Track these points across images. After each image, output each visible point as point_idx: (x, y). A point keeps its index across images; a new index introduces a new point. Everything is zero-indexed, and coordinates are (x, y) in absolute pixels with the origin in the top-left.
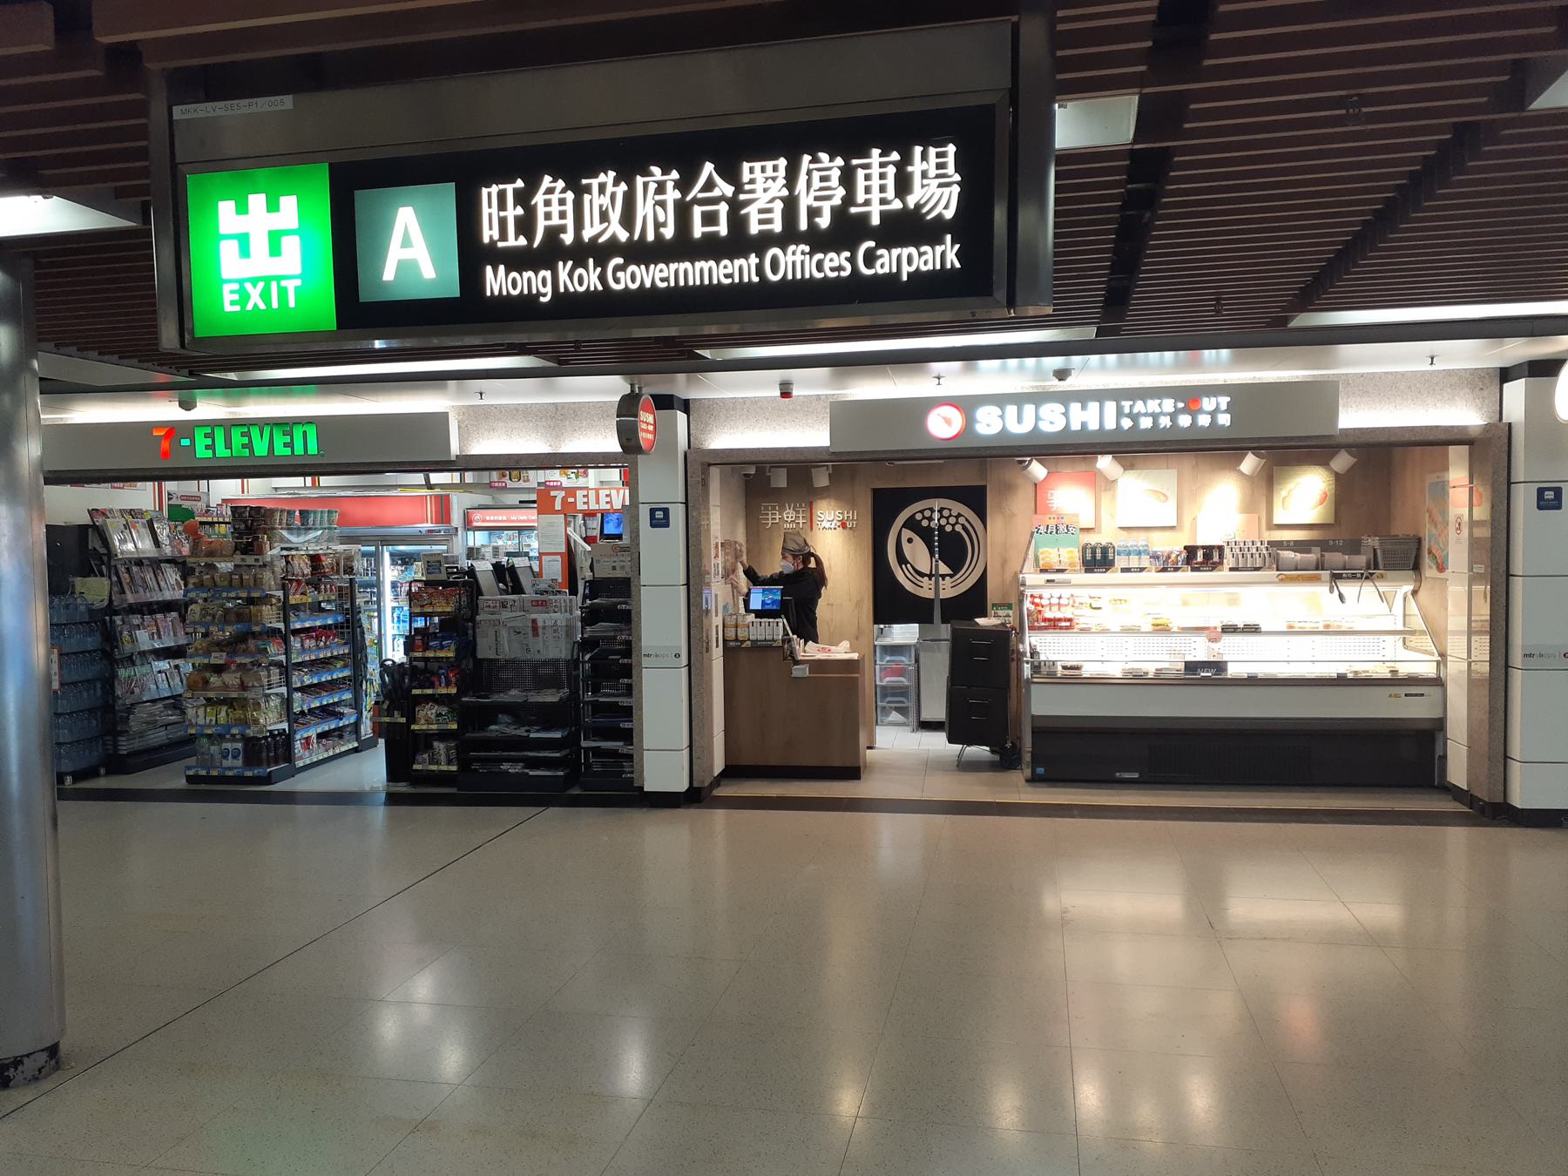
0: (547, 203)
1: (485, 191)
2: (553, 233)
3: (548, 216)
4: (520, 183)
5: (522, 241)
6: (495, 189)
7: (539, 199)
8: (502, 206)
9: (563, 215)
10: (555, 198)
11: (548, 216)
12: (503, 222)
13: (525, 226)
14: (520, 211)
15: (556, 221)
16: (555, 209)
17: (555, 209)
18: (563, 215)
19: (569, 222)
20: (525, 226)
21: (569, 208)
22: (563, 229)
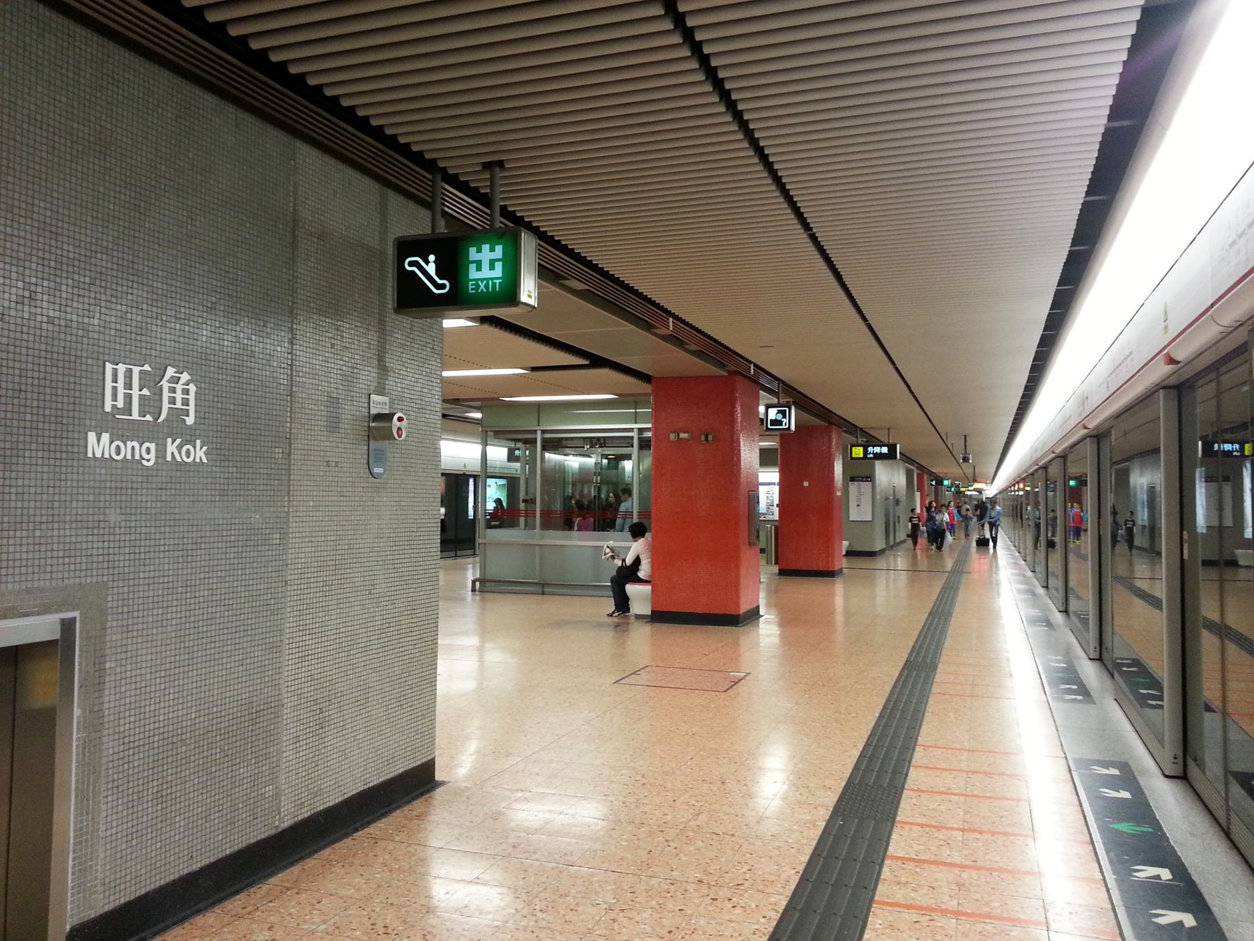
1: (109, 367)
2: (177, 415)
4: (147, 367)
5: (148, 418)
6: (122, 368)
8: (128, 385)
9: (186, 402)
12: (128, 398)
13: (151, 404)
14: (145, 392)
15: (179, 405)
16: (179, 396)
17: (179, 396)
18: (186, 402)
19: (192, 408)
20: (151, 404)
21: (192, 397)
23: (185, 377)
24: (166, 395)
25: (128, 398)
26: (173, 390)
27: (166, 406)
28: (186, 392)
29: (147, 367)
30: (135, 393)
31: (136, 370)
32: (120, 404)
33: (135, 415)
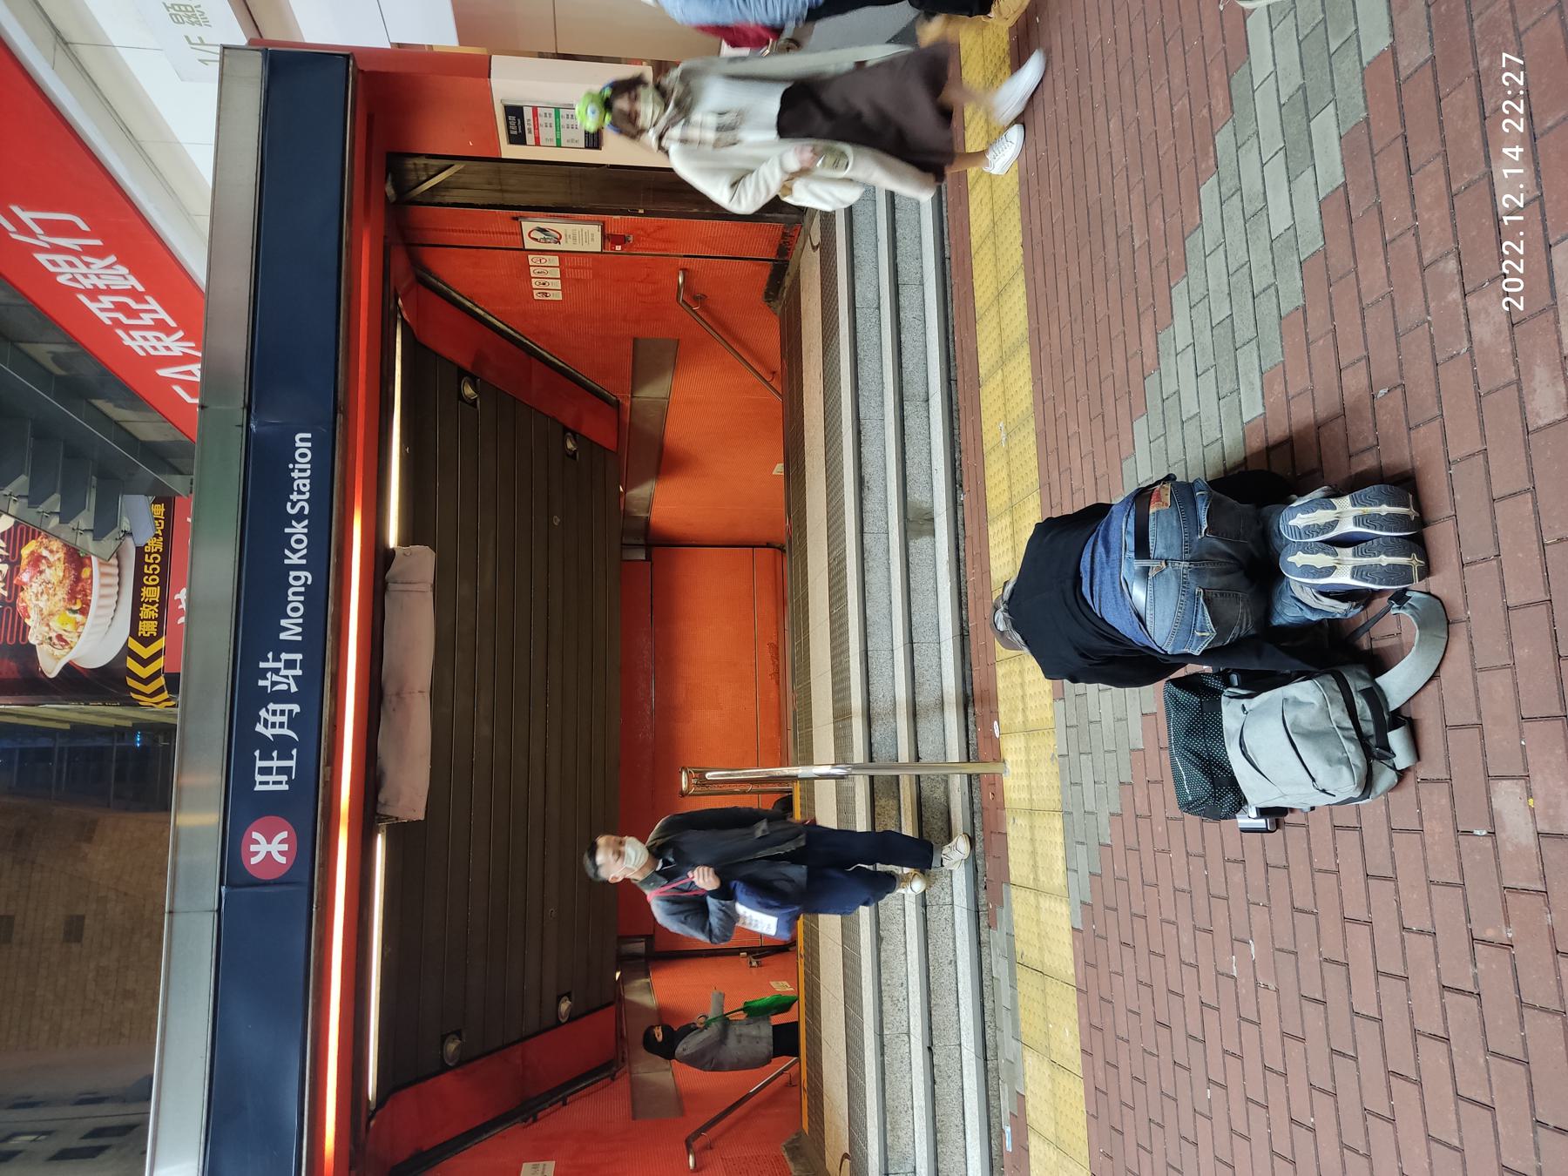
0: (274, 725)
1: (258, 788)
3: (282, 725)
4: (257, 753)
5: (294, 752)
6: (258, 778)
7: (269, 733)
9: (282, 713)
10: (271, 719)
11: (282, 725)
12: (281, 771)
14: (275, 754)
15: (285, 719)
16: (278, 719)
17: (278, 719)
18: (282, 713)
19: (286, 707)
21: (279, 707)
22: (291, 711)
23: (263, 713)
24: (278, 731)
25: (281, 771)
26: (274, 725)
27: (286, 732)
28: (274, 712)
29: (257, 753)
30: (275, 764)
31: (259, 764)
32: (284, 778)
33: (292, 763)
